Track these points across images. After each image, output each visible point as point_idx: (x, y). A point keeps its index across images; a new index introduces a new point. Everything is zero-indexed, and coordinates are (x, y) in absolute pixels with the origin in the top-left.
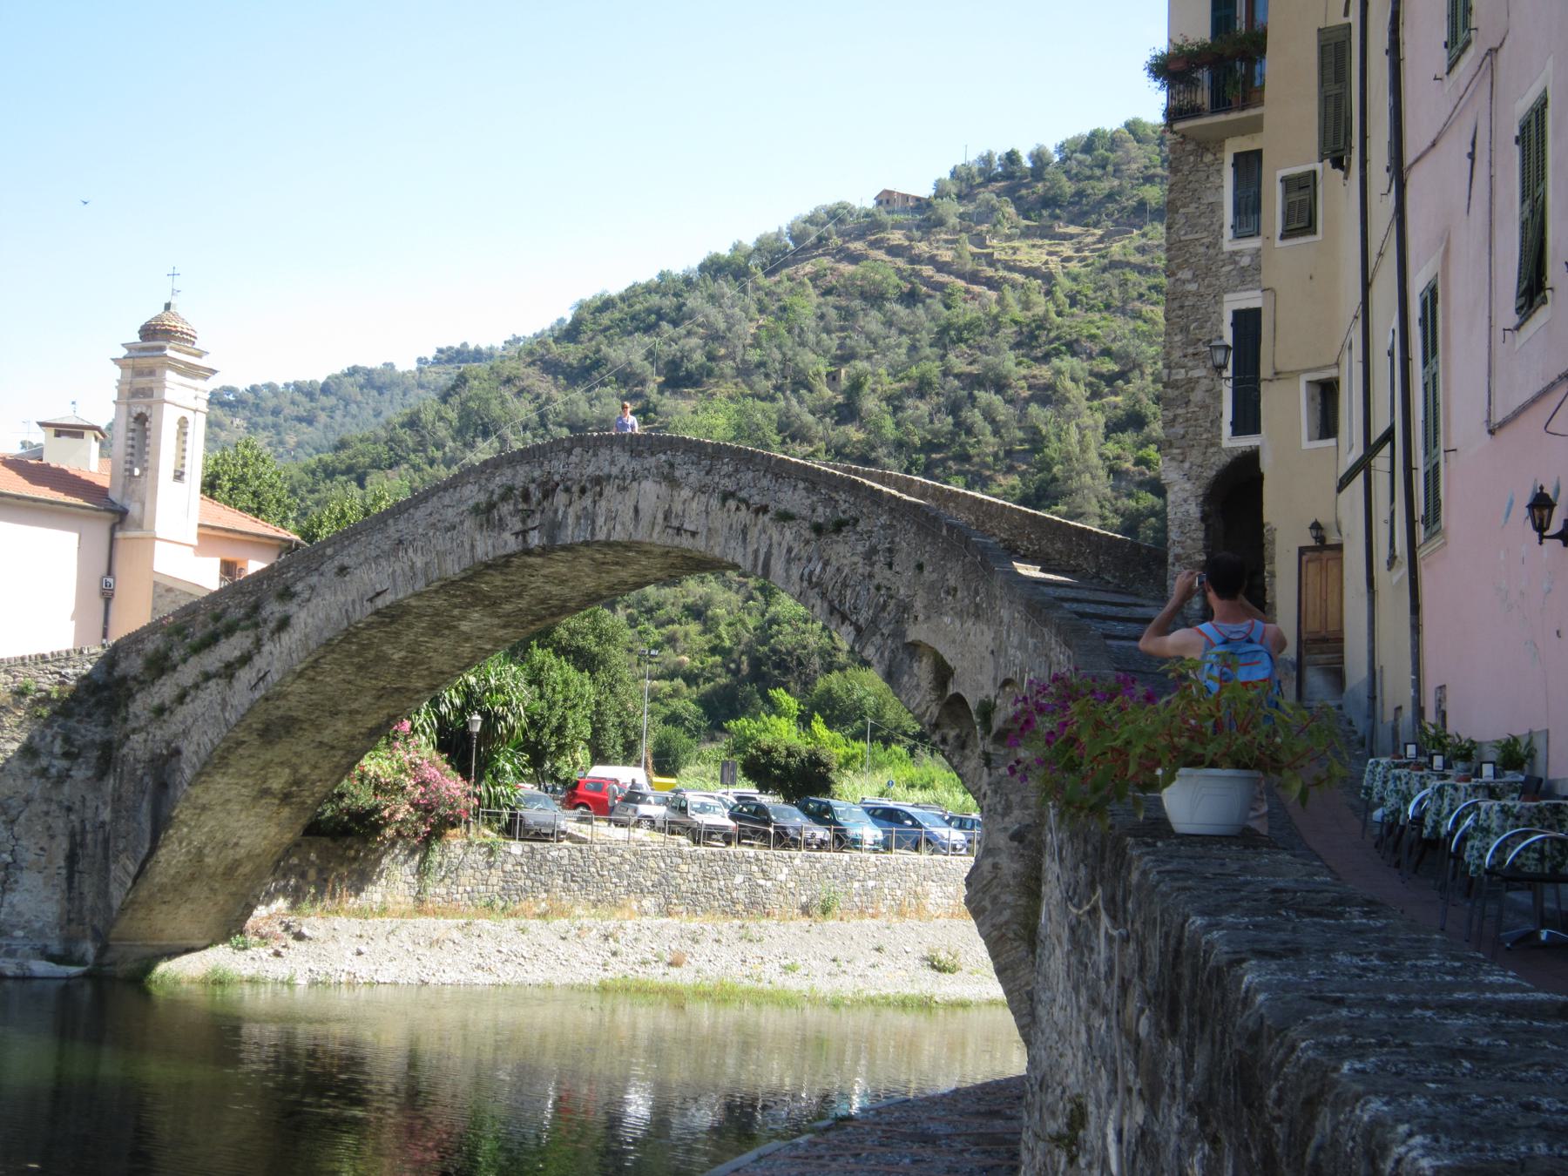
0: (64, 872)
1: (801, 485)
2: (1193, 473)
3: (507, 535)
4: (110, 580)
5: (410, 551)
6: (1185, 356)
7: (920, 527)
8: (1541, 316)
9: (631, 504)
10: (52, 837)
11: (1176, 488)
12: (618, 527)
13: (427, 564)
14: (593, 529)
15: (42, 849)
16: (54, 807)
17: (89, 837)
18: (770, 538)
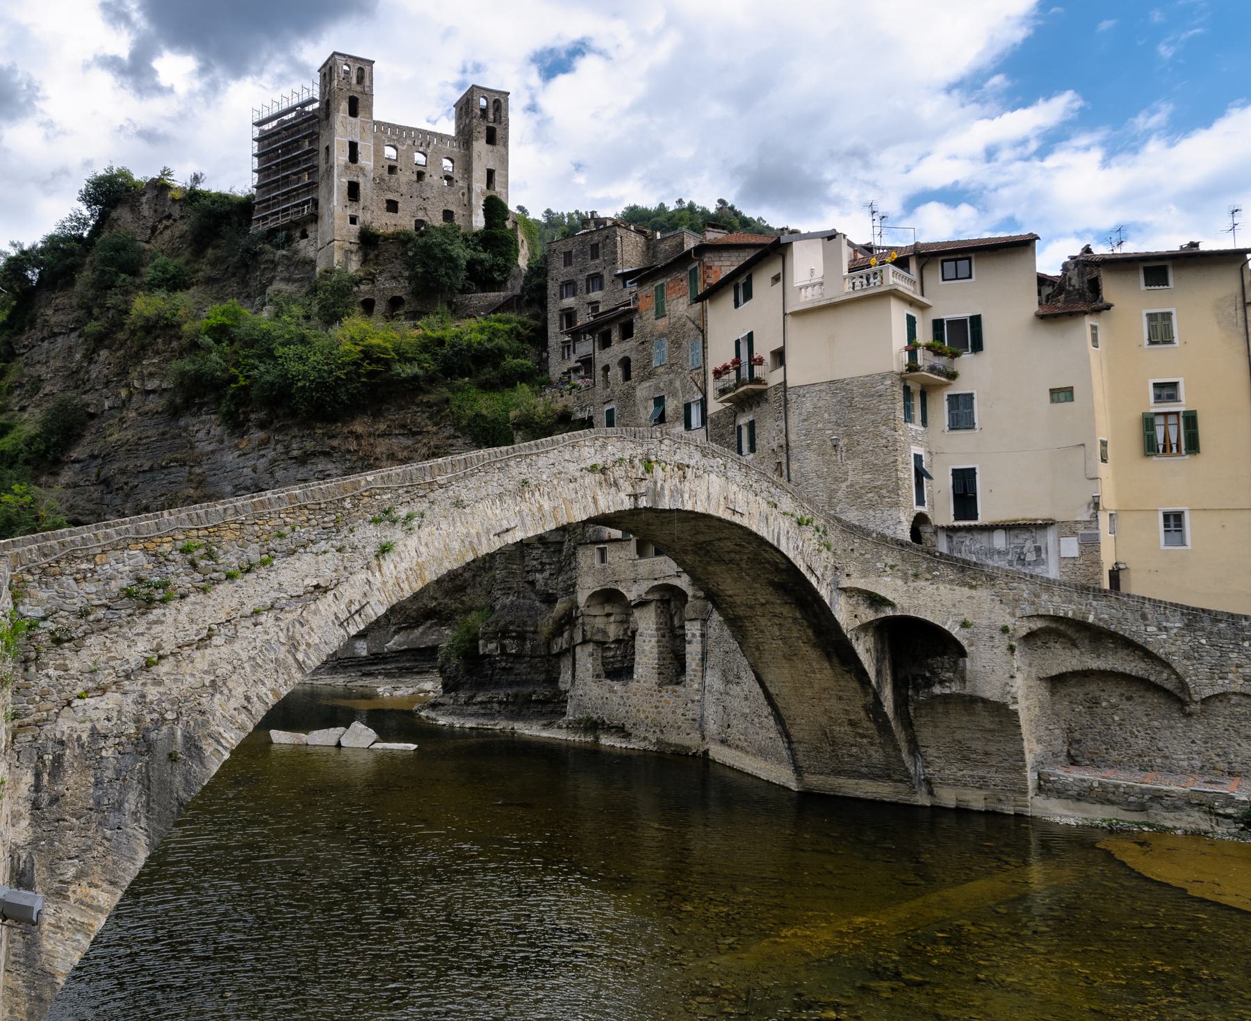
3: (622, 495)
5: (537, 494)
12: (699, 503)
13: (555, 508)
14: (683, 501)
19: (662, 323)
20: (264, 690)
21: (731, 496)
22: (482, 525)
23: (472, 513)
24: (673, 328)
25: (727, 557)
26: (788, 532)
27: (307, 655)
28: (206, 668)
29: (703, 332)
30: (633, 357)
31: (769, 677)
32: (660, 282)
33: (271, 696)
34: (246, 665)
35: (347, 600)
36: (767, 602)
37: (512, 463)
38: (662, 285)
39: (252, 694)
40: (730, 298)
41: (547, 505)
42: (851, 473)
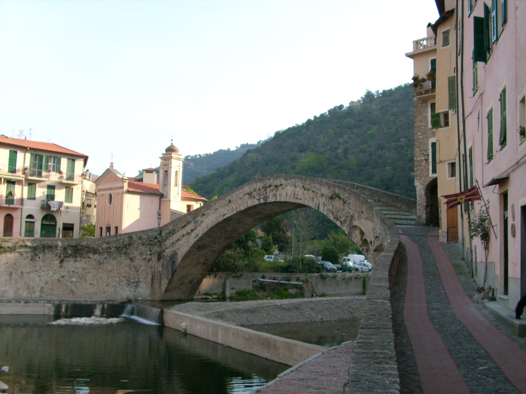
0: (150, 283)
1: (326, 187)
2: (423, 183)
4: (160, 211)
5: (232, 204)
6: (420, 154)
7: (356, 197)
8: (492, 162)
9: (285, 192)
10: (147, 275)
11: (418, 187)
12: (282, 198)
13: (236, 207)
14: (276, 198)
15: (145, 278)
16: (148, 267)
17: (156, 275)
18: (319, 200)
21: (296, 193)
26: (324, 203)
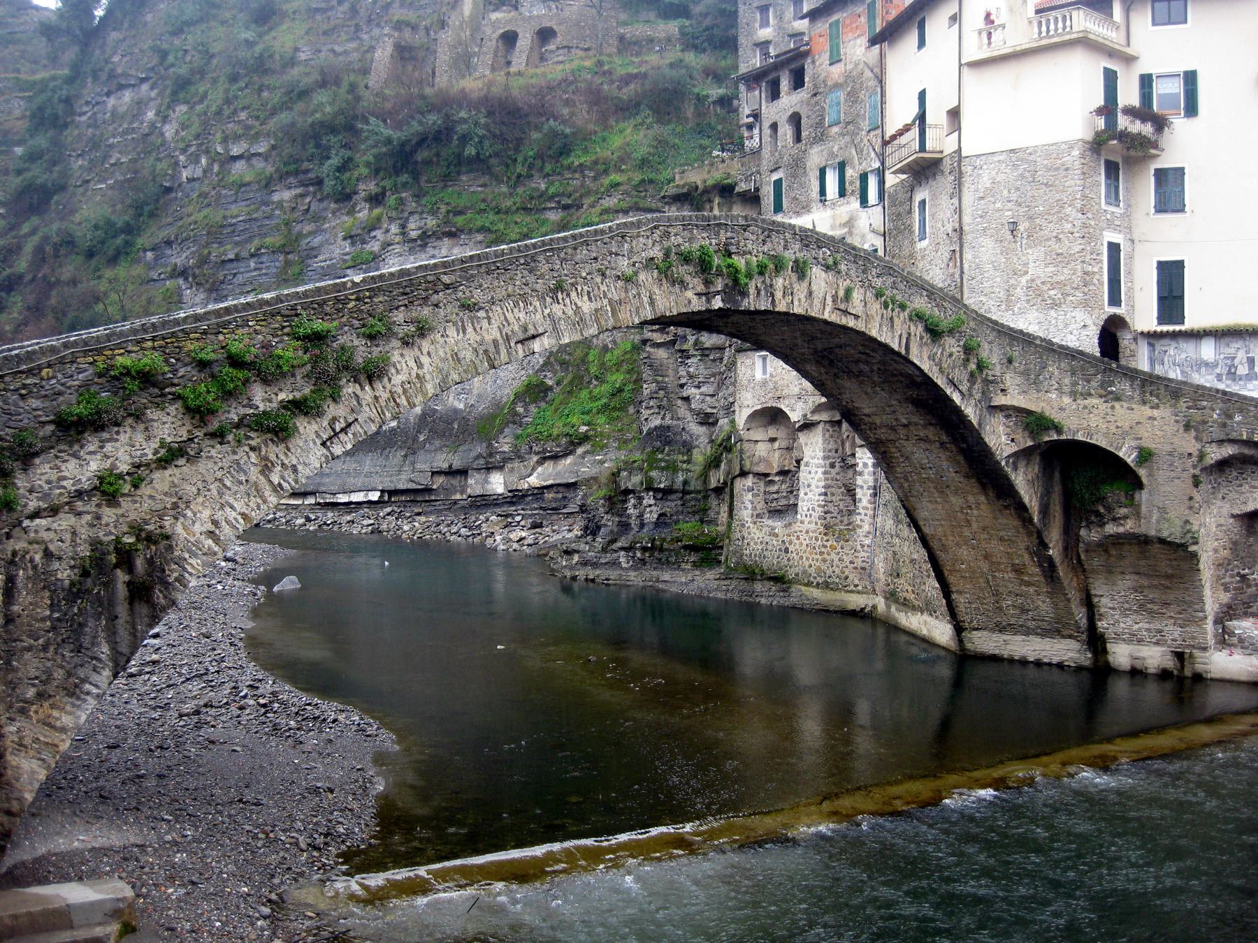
5: (573, 294)
12: (796, 303)
13: (596, 310)
14: (773, 301)
19: (837, 71)
20: (234, 514)
22: (501, 333)
23: (489, 318)
24: (848, 76)
25: (854, 369)
27: (283, 477)
28: (166, 490)
29: (881, 81)
30: (804, 113)
31: (922, 514)
32: (834, 18)
33: (242, 521)
34: (212, 487)
35: (330, 417)
36: (910, 423)
37: (541, 258)
38: (837, 22)
39: (219, 516)
40: (912, 38)
41: (587, 307)
42: (1031, 265)
